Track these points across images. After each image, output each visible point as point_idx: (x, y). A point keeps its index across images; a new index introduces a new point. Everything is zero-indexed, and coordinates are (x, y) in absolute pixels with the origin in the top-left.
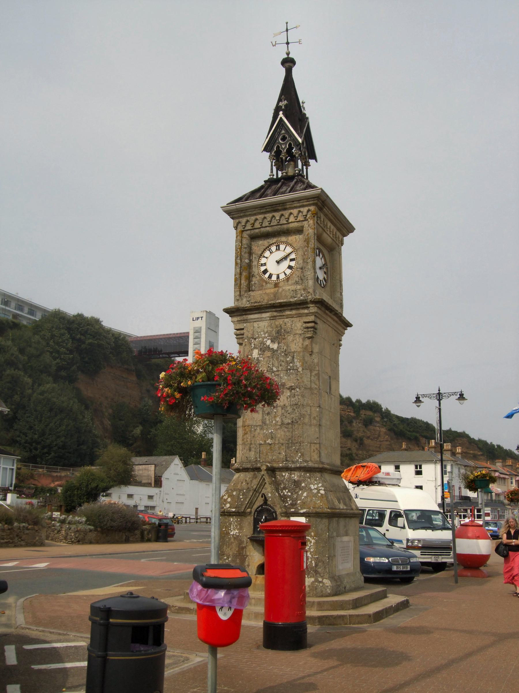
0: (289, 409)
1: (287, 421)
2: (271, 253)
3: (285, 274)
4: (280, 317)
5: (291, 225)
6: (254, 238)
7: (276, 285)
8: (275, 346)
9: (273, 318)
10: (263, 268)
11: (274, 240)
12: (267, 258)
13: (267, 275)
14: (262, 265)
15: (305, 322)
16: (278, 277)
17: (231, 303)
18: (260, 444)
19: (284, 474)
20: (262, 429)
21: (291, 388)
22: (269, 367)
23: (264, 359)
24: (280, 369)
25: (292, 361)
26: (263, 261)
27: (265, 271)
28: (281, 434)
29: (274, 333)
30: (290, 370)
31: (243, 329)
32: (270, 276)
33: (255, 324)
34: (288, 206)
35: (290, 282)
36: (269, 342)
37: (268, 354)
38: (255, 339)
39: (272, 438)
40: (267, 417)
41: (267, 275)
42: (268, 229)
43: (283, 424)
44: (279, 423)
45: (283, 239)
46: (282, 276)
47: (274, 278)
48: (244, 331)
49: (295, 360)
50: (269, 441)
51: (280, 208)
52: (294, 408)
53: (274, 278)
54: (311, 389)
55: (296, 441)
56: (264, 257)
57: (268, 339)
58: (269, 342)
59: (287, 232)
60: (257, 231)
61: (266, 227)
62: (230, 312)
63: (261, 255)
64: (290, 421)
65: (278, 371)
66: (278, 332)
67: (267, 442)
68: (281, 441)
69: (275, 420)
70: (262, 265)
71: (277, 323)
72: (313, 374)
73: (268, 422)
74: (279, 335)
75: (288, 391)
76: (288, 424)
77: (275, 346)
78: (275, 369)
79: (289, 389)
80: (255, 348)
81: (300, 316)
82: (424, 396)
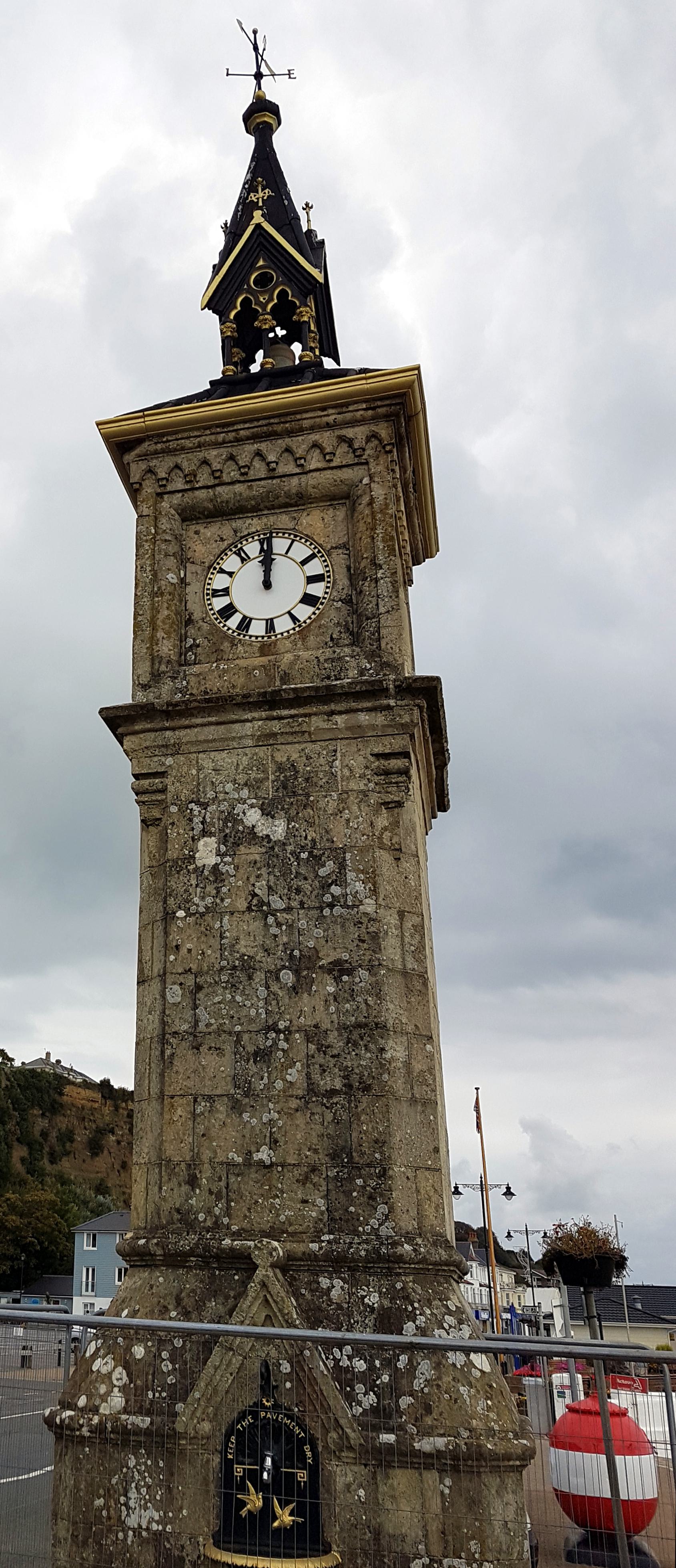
0: (335, 1040)
1: (326, 1083)
2: (243, 560)
3: (294, 619)
4: (290, 739)
5: (311, 480)
6: (190, 515)
7: (266, 649)
8: (278, 829)
9: (267, 739)
10: (219, 603)
11: (255, 524)
12: (231, 574)
13: (234, 622)
14: (216, 593)
15: (378, 756)
16: (270, 624)
17: (122, 694)
19: (324, 1282)
20: (236, 1107)
21: (339, 969)
22: (254, 895)
23: (237, 868)
24: (295, 904)
25: (340, 880)
26: (219, 582)
27: (228, 611)
28: (304, 1134)
30: (331, 906)
31: (162, 774)
32: (246, 623)
33: (206, 761)
34: (306, 424)
35: (312, 640)
36: (253, 817)
37: (253, 853)
38: (205, 806)
39: (274, 1143)
41: (234, 622)
42: (238, 488)
43: (312, 1089)
45: (284, 520)
46: (283, 625)
47: (257, 629)
48: (168, 781)
49: (351, 875)
50: (264, 1154)
51: (279, 428)
52: (355, 1036)
53: (257, 629)
54: (405, 973)
55: (366, 1159)
56: (222, 571)
57: (252, 806)
58: (253, 817)
59: (300, 501)
60: (202, 494)
61: (232, 483)
62: (117, 720)
63: (213, 567)
64: (338, 1084)
65: (288, 909)
67: (256, 1157)
69: (284, 1080)
70: (216, 593)
71: (281, 757)
72: (408, 924)
74: (289, 792)
75: (329, 979)
76: (333, 1092)
77: (278, 829)
78: (278, 903)
79: (330, 972)
80: (205, 833)
81: (357, 734)
82: (465, 1185)
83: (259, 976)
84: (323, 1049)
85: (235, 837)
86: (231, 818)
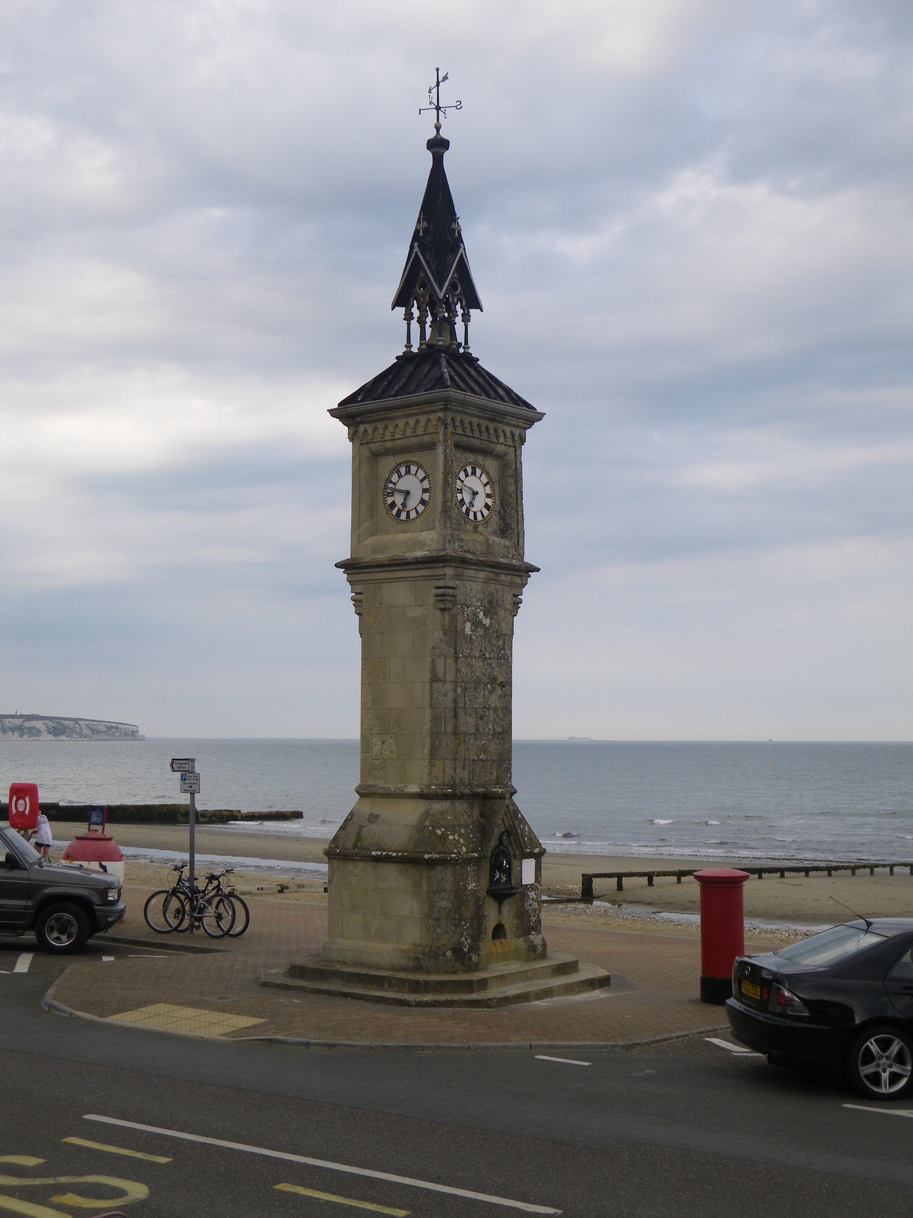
18: (474, 760)
29: (486, 602)
36: (481, 615)
37: (480, 632)
39: (485, 753)
40: (480, 722)
44: (491, 733)
50: (482, 757)
66: (490, 602)
68: (494, 757)
71: (489, 589)
73: (481, 729)
76: (500, 733)
77: (487, 622)
78: (487, 656)
80: (468, 620)
83: (482, 685)
84: (498, 716)
85: (477, 624)
86: (475, 615)
